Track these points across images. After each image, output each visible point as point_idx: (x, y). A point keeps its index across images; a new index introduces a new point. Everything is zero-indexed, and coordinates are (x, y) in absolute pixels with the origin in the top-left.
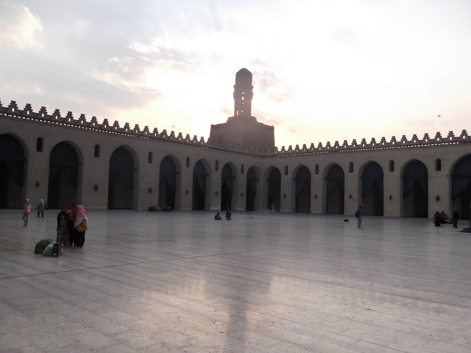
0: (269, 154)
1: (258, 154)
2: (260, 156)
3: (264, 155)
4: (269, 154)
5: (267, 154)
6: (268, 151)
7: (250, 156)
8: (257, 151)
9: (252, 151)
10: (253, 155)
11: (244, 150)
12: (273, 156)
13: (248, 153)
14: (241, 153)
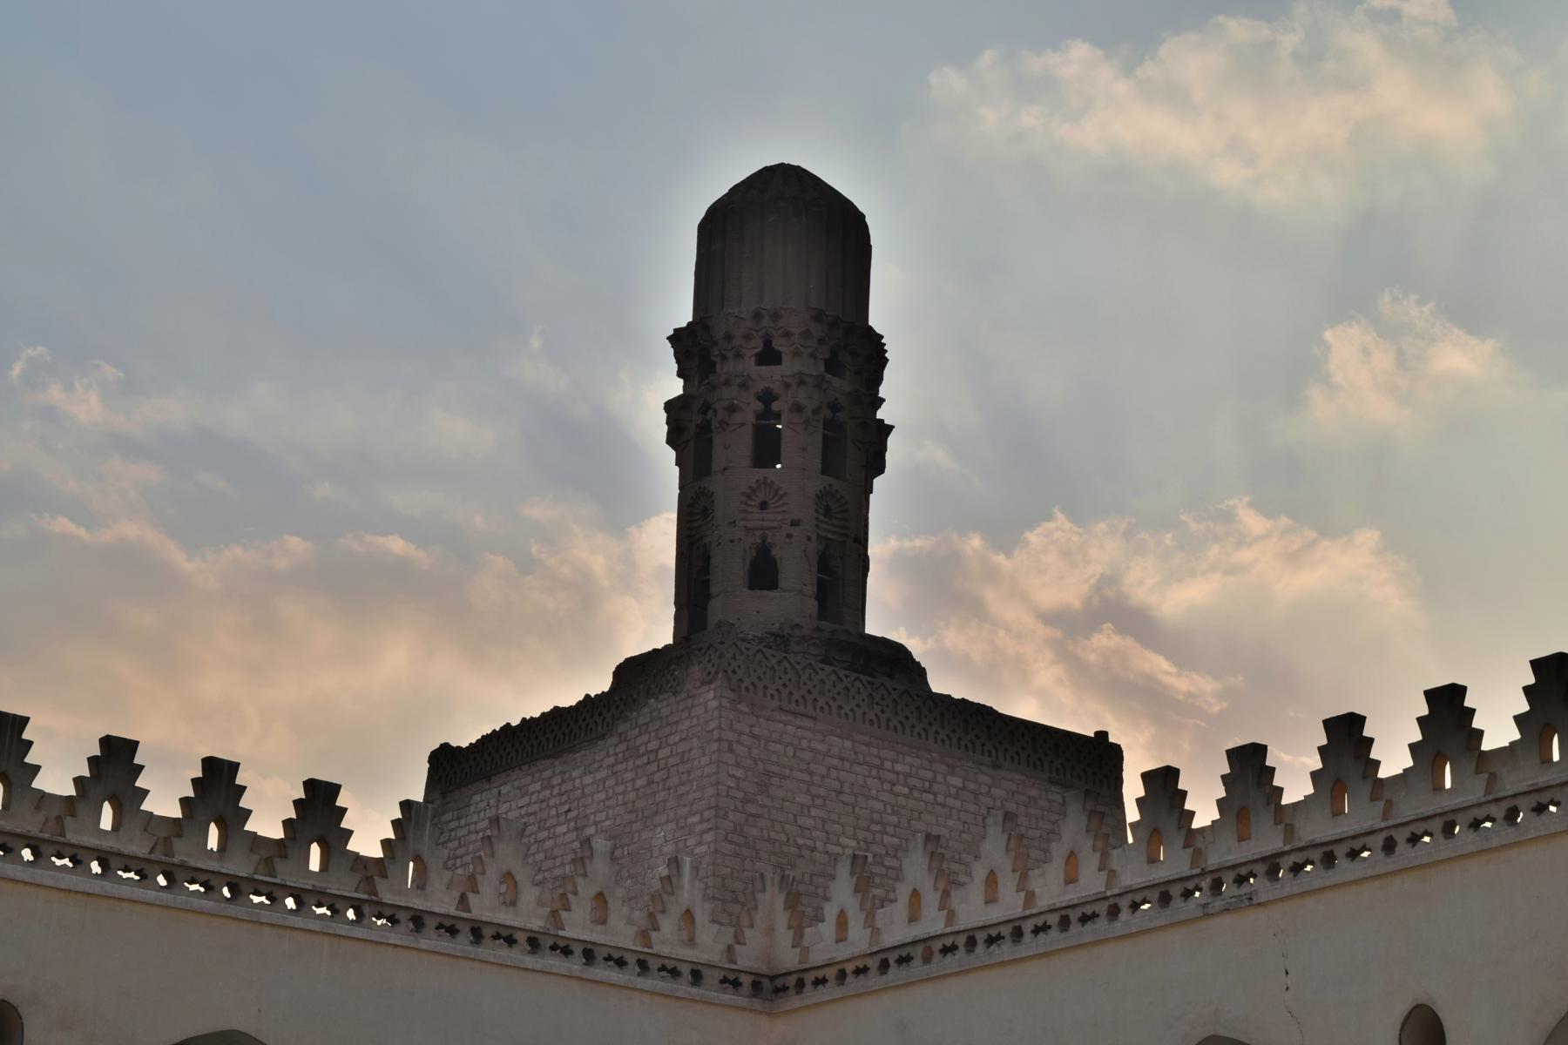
0: (841, 938)
1: (709, 946)
2: (736, 984)
3: (788, 959)
4: (841, 938)
5: (823, 944)
6: (831, 912)
7: (575, 965)
8: (688, 915)
9: (600, 898)
10: (621, 963)
11: (472, 883)
12: (884, 966)
13: (536, 924)
14: (418, 920)
